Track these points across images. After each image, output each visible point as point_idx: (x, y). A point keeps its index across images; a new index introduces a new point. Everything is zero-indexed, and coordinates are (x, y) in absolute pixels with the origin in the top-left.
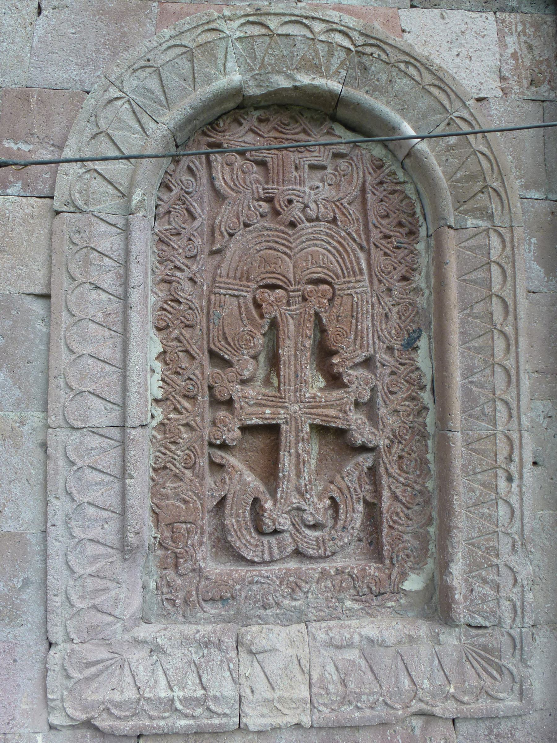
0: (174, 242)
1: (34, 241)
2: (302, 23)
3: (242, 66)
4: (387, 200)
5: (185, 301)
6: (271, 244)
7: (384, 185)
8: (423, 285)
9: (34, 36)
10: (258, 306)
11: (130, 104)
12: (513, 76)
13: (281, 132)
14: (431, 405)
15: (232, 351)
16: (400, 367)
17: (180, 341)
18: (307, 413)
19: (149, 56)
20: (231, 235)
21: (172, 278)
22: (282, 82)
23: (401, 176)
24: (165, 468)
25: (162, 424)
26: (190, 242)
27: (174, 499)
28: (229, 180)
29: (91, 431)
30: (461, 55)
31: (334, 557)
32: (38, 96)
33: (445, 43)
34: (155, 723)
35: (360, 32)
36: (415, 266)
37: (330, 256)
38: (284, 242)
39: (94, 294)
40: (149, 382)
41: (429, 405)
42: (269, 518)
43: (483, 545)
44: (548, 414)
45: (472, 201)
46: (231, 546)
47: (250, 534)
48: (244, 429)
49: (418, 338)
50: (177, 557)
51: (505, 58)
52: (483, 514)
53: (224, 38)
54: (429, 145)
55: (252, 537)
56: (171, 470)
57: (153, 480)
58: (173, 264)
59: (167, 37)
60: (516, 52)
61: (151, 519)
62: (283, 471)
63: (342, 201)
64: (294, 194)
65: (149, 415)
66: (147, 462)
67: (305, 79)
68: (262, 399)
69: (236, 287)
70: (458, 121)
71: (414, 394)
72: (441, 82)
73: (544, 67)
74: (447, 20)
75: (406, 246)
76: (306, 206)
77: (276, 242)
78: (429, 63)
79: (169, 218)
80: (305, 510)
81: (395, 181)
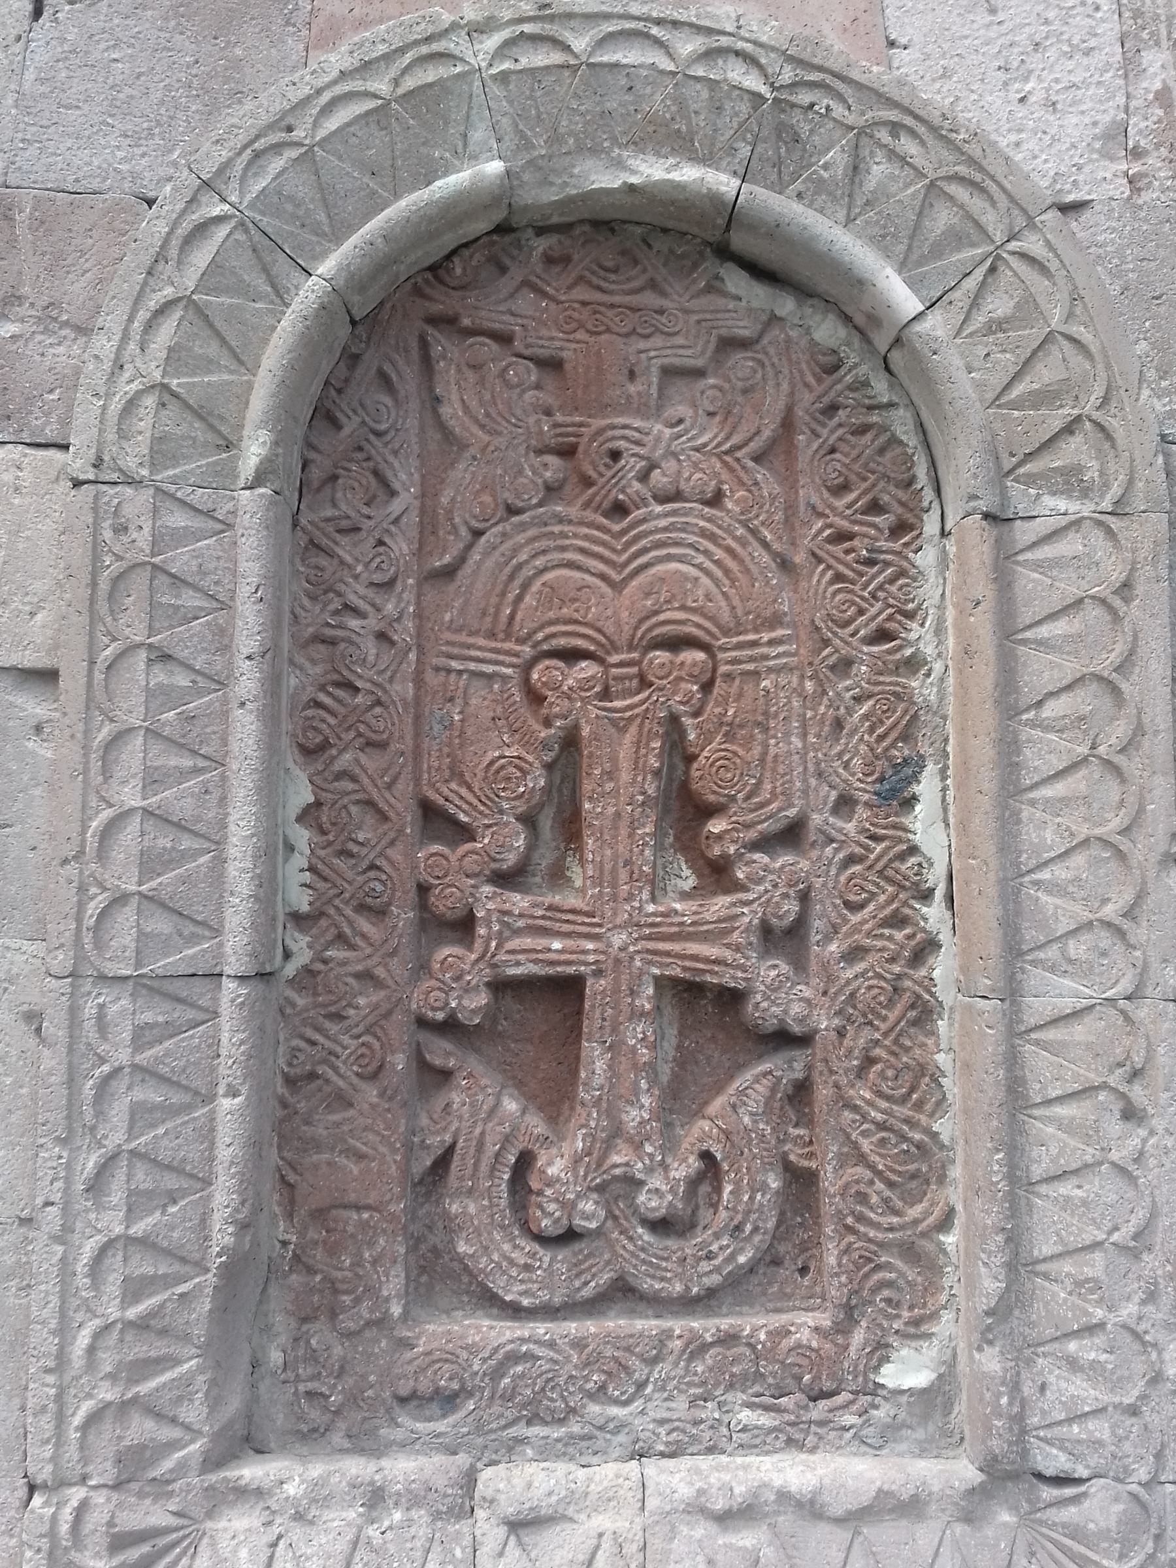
0: (345, 549)
1: (21, 546)
2: (647, 36)
3: (507, 138)
4: (847, 449)
5: (368, 686)
7: (840, 412)
8: (928, 650)
10: (535, 698)
11: (247, 231)
12: (1158, 146)
15: (475, 802)
17: (354, 779)
18: (648, 951)
20: (478, 534)
21: (339, 633)
23: (881, 388)
24: (312, 1076)
25: (308, 971)
26: (381, 549)
28: (473, 404)
29: (145, 986)
30: (1032, 99)
31: (713, 1302)
35: (784, 53)
36: (911, 606)
37: (705, 580)
41: (941, 937)
42: (557, 1200)
43: (1068, 1275)
46: (466, 1268)
48: (501, 987)
49: (915, 778)
50: (336, 1292)
52: (1067, 1199)
54: (946, 322)
56: (327, 1081)
57: (284, 1105)
58: (341, 600)
59: (335, 74)
61: (276, 1197)
63: (739, 454)
64: (624, 438)
65: (280, 951)
66: (271, 1062)
67: (651, 170)
68: (543, 917)
70: (1014, 262)
71: (907, 911)
75: (889, 557)
76: (652, 466)
77: (582, 551)
79: (334, 489)
80: (641, 1183)
81: (867, 401)
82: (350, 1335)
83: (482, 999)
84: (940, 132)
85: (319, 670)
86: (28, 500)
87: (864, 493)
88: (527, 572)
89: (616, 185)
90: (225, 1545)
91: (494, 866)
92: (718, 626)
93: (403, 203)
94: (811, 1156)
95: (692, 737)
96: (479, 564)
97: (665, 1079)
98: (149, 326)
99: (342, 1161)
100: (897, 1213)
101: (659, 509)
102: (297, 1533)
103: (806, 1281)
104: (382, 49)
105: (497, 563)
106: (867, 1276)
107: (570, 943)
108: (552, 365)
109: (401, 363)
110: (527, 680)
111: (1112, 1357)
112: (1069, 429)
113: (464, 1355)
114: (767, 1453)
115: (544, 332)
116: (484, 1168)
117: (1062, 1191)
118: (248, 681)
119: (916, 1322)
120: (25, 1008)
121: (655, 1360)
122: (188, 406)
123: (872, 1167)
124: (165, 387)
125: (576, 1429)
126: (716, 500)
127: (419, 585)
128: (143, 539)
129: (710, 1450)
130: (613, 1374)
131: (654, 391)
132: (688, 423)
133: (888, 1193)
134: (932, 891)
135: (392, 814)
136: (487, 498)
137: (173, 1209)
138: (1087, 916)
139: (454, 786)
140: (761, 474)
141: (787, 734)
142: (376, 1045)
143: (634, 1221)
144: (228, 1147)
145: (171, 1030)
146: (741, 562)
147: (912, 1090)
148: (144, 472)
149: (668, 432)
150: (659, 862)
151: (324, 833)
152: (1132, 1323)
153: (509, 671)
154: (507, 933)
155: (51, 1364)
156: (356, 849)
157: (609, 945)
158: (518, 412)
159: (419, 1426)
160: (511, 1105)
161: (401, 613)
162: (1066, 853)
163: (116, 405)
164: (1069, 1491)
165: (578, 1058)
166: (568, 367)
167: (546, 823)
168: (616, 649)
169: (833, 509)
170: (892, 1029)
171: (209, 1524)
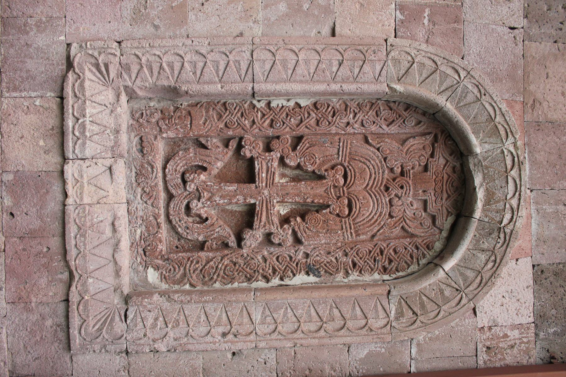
0: (372, 113)
2: (516, 192)
5: (334, 120)
6: (373, 176)
8: (351, 278)
9: (496, 25)
10: (333, 168)
11: (457, 84)
12: (492, 335)
13: (447, 182)
14: (270, 284)
16: (295, 263)
17: (308, 117)
19: (487, 95)
20: (378, 149)
22: (478, 180)
23: (423, 261)
24: (226, 109)
25: (254, 106)
27: (206, 116)
28: (413, 147)
30: (504, 299)
32: (458, 28)
33: (511, 288)
34: (70, 107)
36: (363, 272)
37: (368, 214)
38: (375, 183)
39: (336, 63)
40: (281, 98)
45: (407, 307)
46: (175, 154)
47: (183, 166)
48: (251, 160)
49: (315, 275)
51: (504, 329)
52: (200, 318)
53: (503, 142)
54: (443, 278)
55: (181, 167)
56: (225, 114)
57: (218, 103)
59: (500, 106)
60: (508, 337)
61: (194, 102)
62: (225, 185)
63: (404, 222)
64: (407, 190)
65: (260, 99)
67: (480, 194)
69: (344, 153)
70: (460, 296)
71: (277, 273)
72: (484, 284)
73: (499, 356)
74: (526, 290)
76: (399, 198)
77: (375, 179)
78: (496, 275)
80: (199, 201)
82: (158, 123)
83: (248, 155)
84: (494, 274)
85: (338, 107)
86: (380, 28)
87: (394, 258)
88: (368, 163)
89: (476, 185)
90: (105, 93)
91: (285, 157)
92: (355, 218)
93: (467, 126)
94: (208, 248)
95: (324, 211)
96: (370, 150)
97: (227, 207)
98: (430, 58)
99: (203, 119)
100: (194, 272)
101: (387, 200)
102: (108, 111)
103: (174, 248)
104: (508, 119)
105: (370, 155)
106: (177, 264)
107: (265, 179)
108: (426, 169)
109: (423, 127)
110: (337, 164)
112: (414, 313)
113: (153, 154)
115: (434, 167)
116: (202, 157)
118: (335, 87)
119: (165, 278)
120: (244, 32)
121: (152, 206)
122: (409, 69)
123: (206, 265)
124: (414, 63)
125: (134, 185)
127: (363, 134)
128: (372, 58)
129: (130, 222)
130: (148, 195)
131: (420, 198)
132: (412, 207)
133: (199, 269)
134: (283, 280)
135: (298, 128)
136: (388, 152)
137: (191, 73)
138: (278, 322)
139: (308, 145)
140: (398, 229)
142: (235, 126)
143: (189, 200)
144: (208, 88)
145: (239, 70)
146: (373, 224)
147: (227, 276)
148: (390, 57)
149: (409, 202)
150: (288, 204)
151: (293, 110)
154: (267, 161)
155: (151, 45)
156: (289, 118)
158: (412, 160)
159: (134, 143)
160: (220, 164)
161: (355, 129)
162: (296, 316)
163: (408, 50)
164: (123, 318)
165: (232, 183)
166: (425, 173)
167: (297, 172)
168: (347, 189)
169: (389, 249)
171: (110, 88)
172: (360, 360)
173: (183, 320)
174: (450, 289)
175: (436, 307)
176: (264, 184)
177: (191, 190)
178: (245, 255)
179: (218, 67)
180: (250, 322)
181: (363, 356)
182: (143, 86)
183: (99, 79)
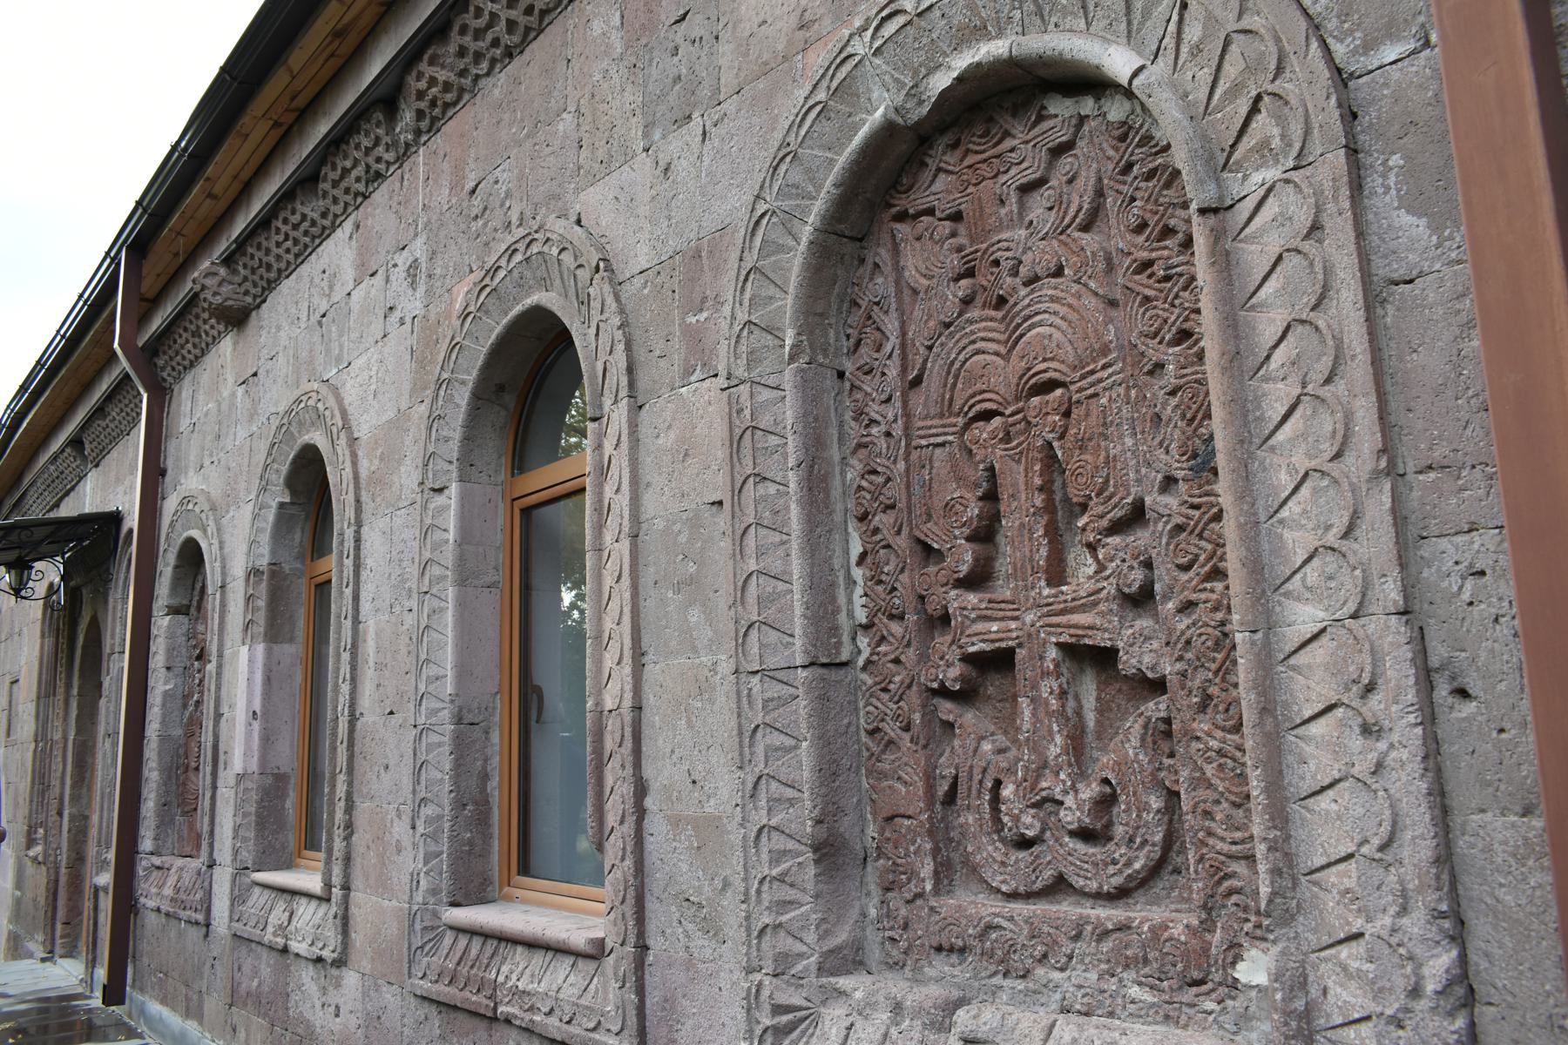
20: (930, 348)
22: (941, 81)
25: (868, 662)
31: (1131, 901)
38: (991, 335)
44: (1471, 565)
45: (1245, 139)
54: (1166, 64)
67: (961, 62)
69: (940, 430)
75: (1178, 269)
77: (983, 339)
88: (957, 365)
99: (898, 785)
100: (1238, 829)
107: (1003, 624)
111: (1371, 967)
112: (1254, 110)
114: (1150, 1024)
116: (974, 792)
117: (1323, 805)
126: (1059, 272)
129: (1111, 1014)
141: (1121, 437)
152: (1385, 934)
153: (950, 438)
157: (1024, 624)
170: (1219, 670)
171: (822, 1010)
172: (1436, 228)
173: (1338, 875)
174: (1186, 29)
175: (1233, 48)
176: (1013, 625)
177: (1038, 825)
178: (1178, 666)
179: (777, 749)
180: (1324, 639)
181: (1423, 222)
182: (817, 927)
183: (804, 1033)
